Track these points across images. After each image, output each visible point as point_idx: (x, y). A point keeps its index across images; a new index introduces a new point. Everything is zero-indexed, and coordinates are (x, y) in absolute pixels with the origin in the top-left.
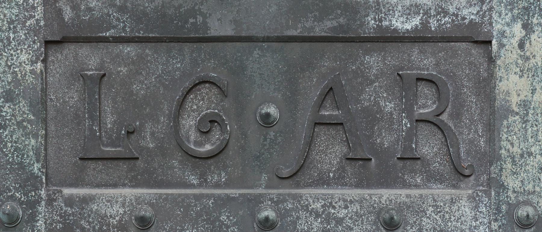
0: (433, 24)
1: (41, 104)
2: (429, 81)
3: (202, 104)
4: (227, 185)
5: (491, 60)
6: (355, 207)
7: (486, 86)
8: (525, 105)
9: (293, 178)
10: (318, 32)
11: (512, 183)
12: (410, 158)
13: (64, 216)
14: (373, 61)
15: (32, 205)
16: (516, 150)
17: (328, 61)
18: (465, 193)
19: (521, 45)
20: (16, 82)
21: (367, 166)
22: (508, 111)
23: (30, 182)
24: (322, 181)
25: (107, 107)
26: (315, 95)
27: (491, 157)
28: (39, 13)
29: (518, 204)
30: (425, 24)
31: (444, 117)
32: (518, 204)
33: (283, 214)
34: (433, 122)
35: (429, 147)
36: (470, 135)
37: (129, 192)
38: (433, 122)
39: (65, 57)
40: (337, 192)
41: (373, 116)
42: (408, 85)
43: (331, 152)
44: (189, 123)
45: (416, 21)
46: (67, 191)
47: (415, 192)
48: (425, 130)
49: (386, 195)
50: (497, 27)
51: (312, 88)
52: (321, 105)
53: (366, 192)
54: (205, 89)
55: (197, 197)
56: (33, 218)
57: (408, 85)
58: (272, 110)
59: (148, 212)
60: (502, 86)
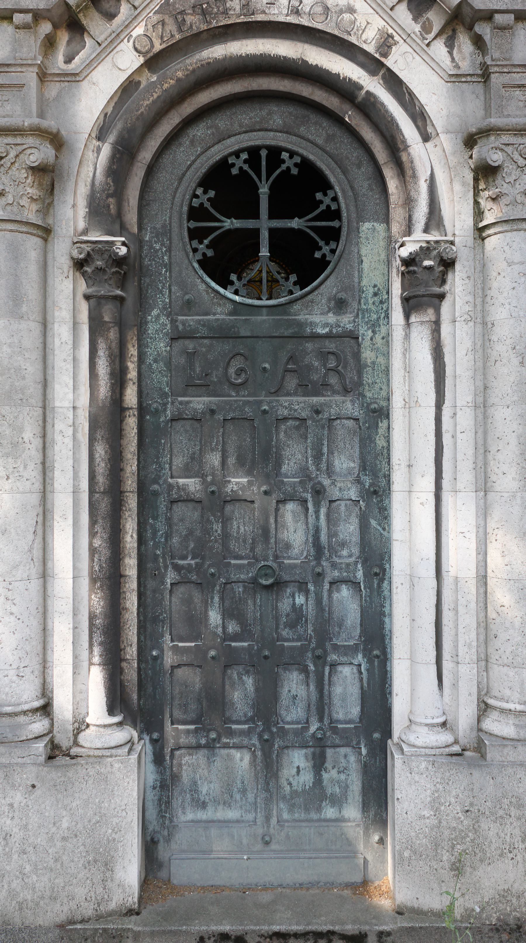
0: (334, 331)
1: (168, 364)
2: (333, 353)
3: (237, 363)
4: (248, 396)
5: (359, 345)
6: (302, 405)
7: (357, 355)
8: (373, 363)
9: (276, 393)
10: (286, 334)
11: (369, 395)
12: (325, 385)
13: (178, 409)
14: (309, 346)
15: (165, 404)
16: (370, 381)
17: (290, 346)
18: (348, 399)
19: (371, 339)
20: (158, 355)
21: (308, 388)
22: (366, 366)
23: (164, 395)
24: (288, 394)
25: (197, 365)
26: (285, 360)
27: (359, 384)
28: (169, 326)
29: (371, 403)
30: (331, 331)
31: (340, 368)
32: (371, 403)
33: (272, 408)
34: (335, 370)
35: (333, 380)
36: (351, 375)
37: (206, 399)
38: (335, 370)
39: (179, 345)
40: (295, 399)
41: (309, 368)
42: (324, 356)
43: (292, 383)
44: (232, 371)
45: (327, 330)
46: (180, 399)
47: (327, 398)
48: (331, 373)
49: (315, 400)
50: (361, 332)
51: (284, 356)
52: (287, 363)
53: (307, 399)
54: (238, 357)
55: (236, 401)
56: (165, 410)
57: (324, 356)
58: (267, 366)
59: (214, 407)
60: (363, 355)
